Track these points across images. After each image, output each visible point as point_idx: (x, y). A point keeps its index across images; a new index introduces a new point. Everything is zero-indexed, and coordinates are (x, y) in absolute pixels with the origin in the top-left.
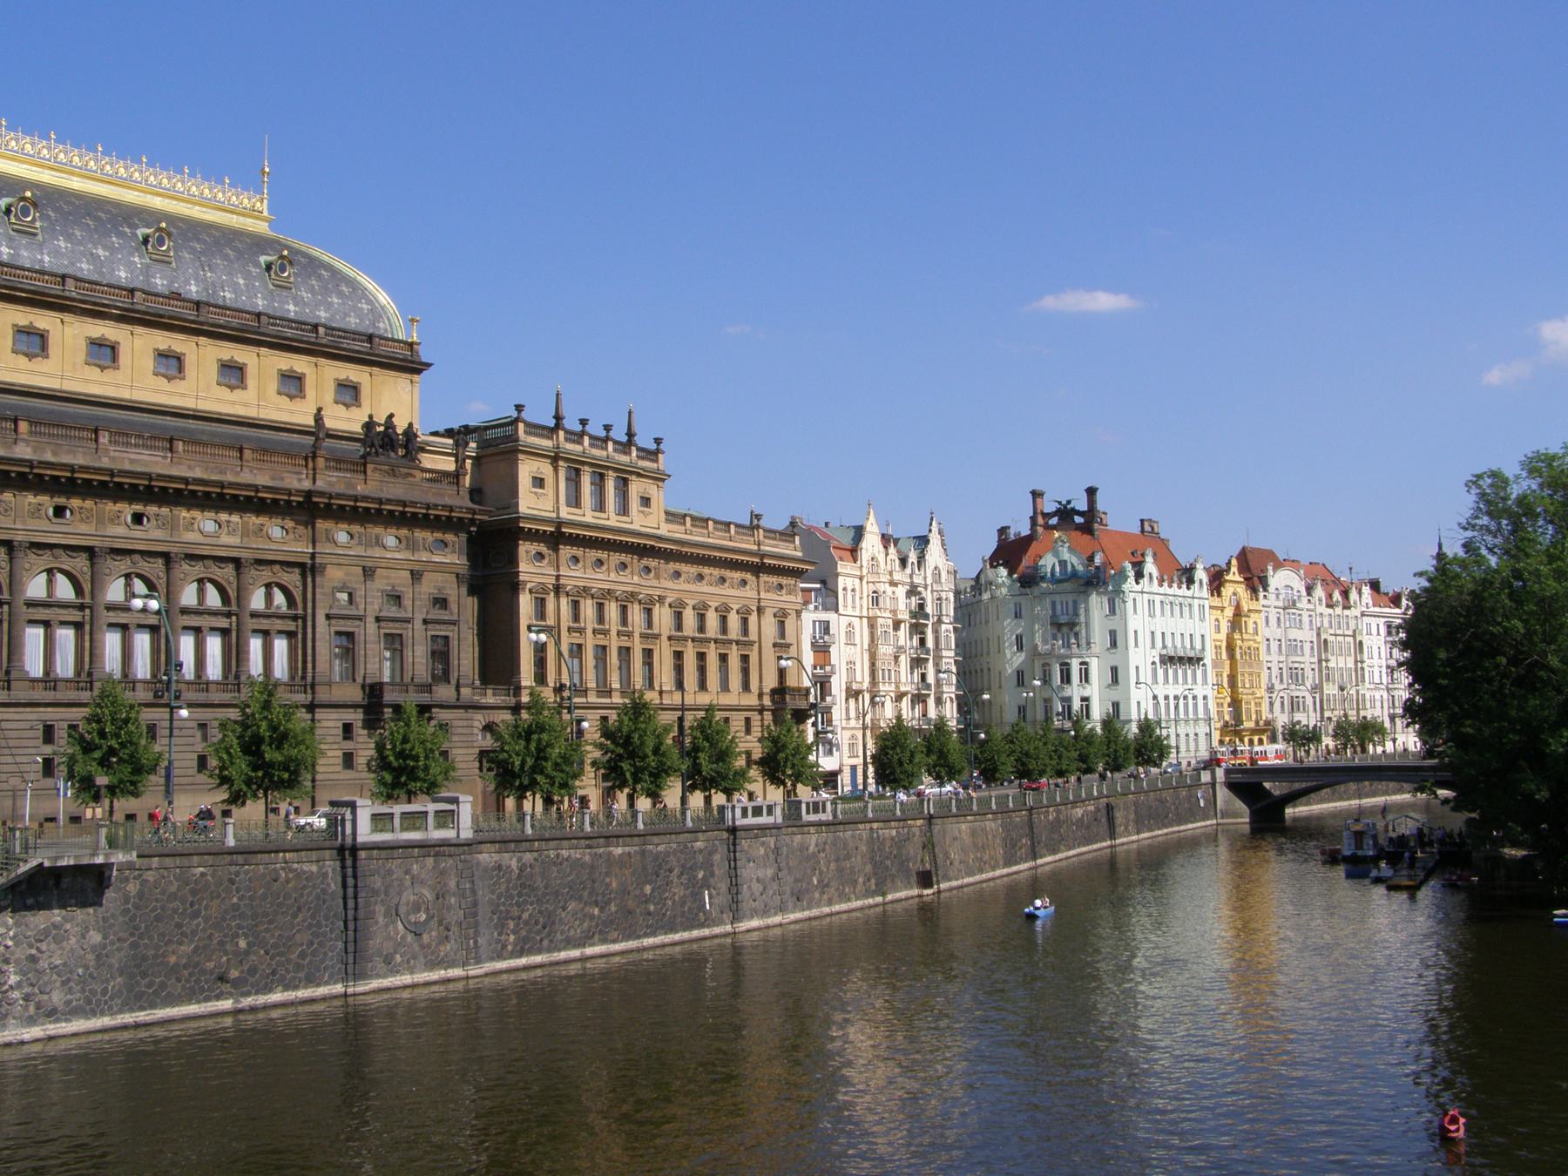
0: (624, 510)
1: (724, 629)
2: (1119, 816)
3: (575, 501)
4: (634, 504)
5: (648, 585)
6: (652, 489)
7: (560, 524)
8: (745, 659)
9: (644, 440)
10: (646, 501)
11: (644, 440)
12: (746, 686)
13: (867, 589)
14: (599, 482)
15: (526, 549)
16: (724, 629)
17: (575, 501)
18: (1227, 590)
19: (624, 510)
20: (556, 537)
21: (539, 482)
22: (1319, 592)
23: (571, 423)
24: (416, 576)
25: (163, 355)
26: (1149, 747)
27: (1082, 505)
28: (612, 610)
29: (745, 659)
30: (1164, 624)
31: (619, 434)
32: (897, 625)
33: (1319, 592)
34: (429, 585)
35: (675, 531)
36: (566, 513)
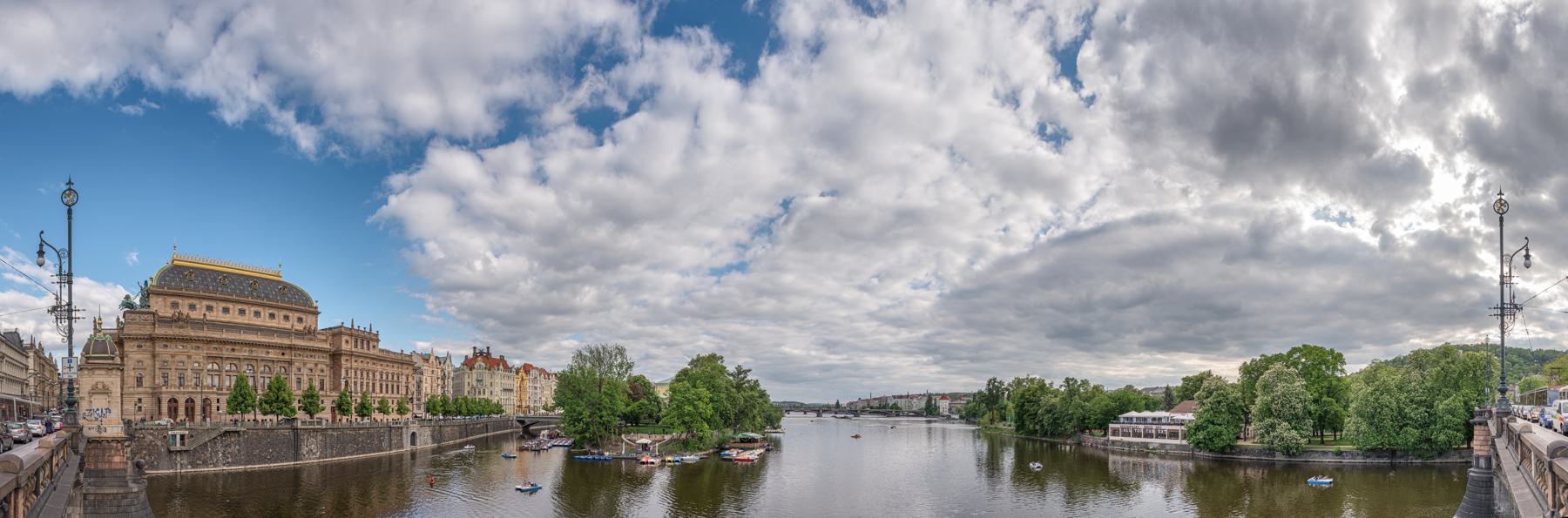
0: (369, 349)
1: (393, 378)
2: (489, 427)
3: (356, 346)
4: (371, 347)
5: (370, 366)
6: (376, 344)
7: (352, 352)
8: (398, 386)
9: (374, 332)
10: (374, 347)
11: (374, 332)
12: (398, 393)
13: (431, 369)
14: (362, 343)
15: (343, 359)
16: (393, 378)
17: (356, 346)
18: (520, 374)
19: (369, 349)
20: (351, 354)
21: (347, 342)
22: (542, 375)
23: (356, 327)
24: (316, 365)
25: (255, 312)
26: (499, 409)
27: (486, 351)
28: (359, 372)
29: (398, 386)
30: (505, 381)
31: (368, 330)
32: (438, 378)
33: (542, 375)
34: (320, 366)
35: (381, 354)
36: (353, 350)
